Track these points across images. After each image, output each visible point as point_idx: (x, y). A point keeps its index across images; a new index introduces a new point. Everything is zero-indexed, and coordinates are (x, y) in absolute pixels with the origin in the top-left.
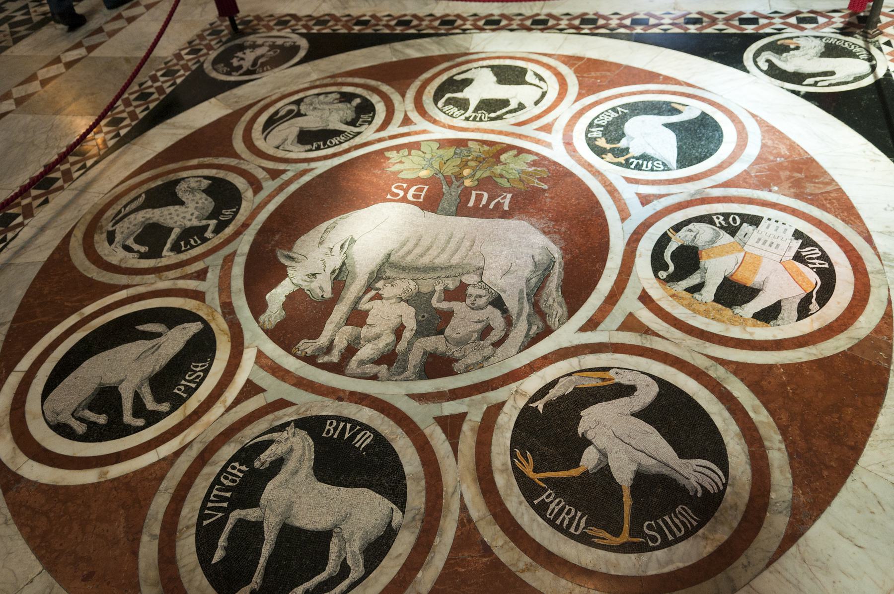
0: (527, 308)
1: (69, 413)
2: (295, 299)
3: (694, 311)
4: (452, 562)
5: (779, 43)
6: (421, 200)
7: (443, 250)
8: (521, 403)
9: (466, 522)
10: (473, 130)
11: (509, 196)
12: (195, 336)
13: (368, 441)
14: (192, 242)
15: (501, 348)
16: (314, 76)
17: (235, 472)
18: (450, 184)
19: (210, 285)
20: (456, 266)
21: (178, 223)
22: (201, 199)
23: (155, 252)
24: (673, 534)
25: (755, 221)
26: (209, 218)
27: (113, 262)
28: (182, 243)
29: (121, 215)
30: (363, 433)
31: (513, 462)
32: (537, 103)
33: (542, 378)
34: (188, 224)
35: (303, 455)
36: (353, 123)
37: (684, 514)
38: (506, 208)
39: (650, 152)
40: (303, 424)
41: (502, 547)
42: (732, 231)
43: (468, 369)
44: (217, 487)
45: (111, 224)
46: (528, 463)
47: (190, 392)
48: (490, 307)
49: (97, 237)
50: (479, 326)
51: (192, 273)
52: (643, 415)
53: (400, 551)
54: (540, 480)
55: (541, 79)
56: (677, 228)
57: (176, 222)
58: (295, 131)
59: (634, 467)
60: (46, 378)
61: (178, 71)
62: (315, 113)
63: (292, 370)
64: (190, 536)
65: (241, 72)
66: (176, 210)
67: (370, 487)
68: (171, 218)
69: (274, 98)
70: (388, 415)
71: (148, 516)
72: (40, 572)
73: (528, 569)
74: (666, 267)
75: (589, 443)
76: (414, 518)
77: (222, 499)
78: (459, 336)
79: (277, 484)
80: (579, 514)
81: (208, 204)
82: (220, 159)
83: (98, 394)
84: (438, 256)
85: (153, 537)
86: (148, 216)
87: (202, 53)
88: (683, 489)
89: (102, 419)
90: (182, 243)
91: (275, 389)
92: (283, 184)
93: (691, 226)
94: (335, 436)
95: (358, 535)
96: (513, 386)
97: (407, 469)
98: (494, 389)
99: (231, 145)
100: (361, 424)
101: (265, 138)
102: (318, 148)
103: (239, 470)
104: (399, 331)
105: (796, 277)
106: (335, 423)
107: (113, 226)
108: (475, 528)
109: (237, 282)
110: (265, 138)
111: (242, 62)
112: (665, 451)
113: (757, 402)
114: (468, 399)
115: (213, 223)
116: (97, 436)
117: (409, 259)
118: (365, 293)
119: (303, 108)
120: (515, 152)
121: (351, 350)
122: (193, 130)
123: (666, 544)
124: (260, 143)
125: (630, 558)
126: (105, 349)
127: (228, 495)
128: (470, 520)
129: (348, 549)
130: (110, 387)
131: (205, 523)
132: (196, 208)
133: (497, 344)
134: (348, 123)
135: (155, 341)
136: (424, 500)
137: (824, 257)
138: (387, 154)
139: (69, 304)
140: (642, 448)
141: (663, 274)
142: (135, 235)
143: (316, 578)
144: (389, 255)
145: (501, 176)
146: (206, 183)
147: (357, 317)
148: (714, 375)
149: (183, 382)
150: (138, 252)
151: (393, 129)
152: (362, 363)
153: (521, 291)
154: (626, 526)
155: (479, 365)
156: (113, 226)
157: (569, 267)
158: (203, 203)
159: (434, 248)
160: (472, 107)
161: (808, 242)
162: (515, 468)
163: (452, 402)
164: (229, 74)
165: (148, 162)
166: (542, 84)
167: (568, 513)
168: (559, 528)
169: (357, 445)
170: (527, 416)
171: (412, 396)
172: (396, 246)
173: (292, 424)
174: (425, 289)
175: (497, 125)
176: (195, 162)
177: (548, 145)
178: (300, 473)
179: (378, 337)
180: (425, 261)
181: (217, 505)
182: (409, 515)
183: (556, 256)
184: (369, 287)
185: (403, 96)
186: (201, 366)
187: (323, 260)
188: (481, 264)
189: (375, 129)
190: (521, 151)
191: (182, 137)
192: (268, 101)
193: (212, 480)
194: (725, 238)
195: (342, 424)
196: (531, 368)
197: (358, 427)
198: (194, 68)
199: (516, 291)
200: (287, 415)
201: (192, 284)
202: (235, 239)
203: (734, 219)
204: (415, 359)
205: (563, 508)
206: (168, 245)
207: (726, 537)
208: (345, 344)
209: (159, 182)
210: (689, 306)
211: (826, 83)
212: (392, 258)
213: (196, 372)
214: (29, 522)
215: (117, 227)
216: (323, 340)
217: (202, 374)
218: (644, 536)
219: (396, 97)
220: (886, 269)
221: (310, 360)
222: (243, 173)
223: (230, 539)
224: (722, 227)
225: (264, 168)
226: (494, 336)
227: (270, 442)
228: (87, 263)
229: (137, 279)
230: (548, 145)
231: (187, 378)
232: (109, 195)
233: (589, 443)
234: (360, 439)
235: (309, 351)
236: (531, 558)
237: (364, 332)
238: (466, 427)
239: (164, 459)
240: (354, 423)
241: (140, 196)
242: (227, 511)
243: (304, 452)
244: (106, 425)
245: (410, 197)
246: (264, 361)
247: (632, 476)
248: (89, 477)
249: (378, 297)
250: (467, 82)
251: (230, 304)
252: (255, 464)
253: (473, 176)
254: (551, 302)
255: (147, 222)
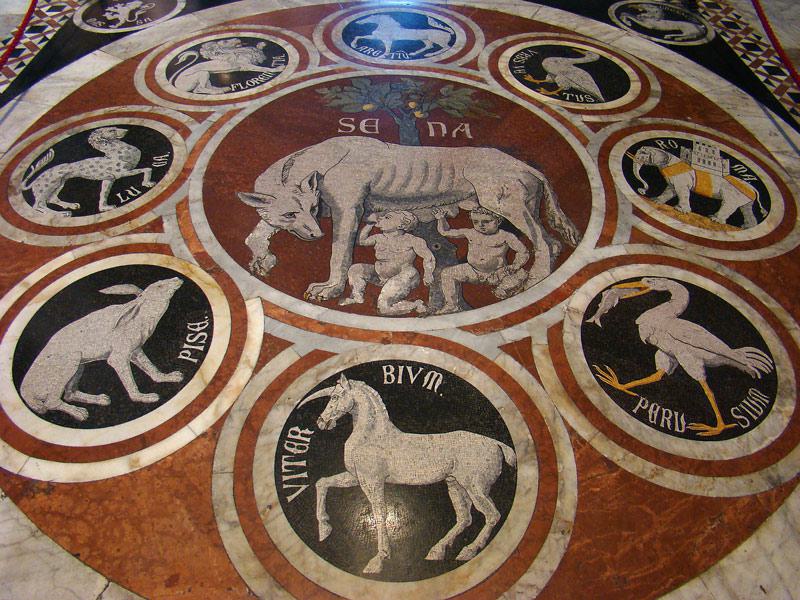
0: (538, 228)
1: (60, 395)
2: (282, 241)
3: (680, 220)
4: (584, 484)
5: (630, 6)
6: (377, 132)
7: (425, 179)
8: (579, 321)
9: (578, 443)
10: (400, 68)
11: (467, 125)
12: (177, 293)
13: (439, 381)
14: (130, 193)
15: (532, 271)
16: (204, 25)
17: (299, 437)
18: (400, 116)
19: (170, 233)
20: (447, 194)
21: (105, 175)
22: (122, 148)
23: (90, 208)
24: (757, 415)
25: (689, 144)
26: (139, 166)
27: (42, 224)
28: (119, 195)
29: (32, 174)
30: (429, 374)
31: (597, 378)
32: (451, 43)
33: (586, 294)
34: (118, 175)
35: (371, 407)
36: (266, 64)
37: (755, 399)
38: (470, 137)
39: (574, 86)
40: (358, 373)
41: (624, 459)
42: (677, 153)
43: (510, 293)
44: (284, 457)
45: (24, 183)
46: (609, 374)
47: (201, 356)
48: (501, 231)
49: (12, 199)
50: (500, 251)
51: (145, 226)
52: (686, 315)
53: (528, 487)
54: (629, 389)
55: (444, 25)
56: (633, 149)
57: (102, 174)
58: (204, 78)
59: (702, 364)
60: (11, 361)
61: (45, 27)
62: (219, 57)
63: (314, 317)
64: (277, 516)
65: (118, 25)
66: (98, 162)
67: (464, 429)
68: (94, 171)
69: (167, 46)
70: (448, 351)
71: (214, 502)
72: (107, 586)
73: (656, 473)
74: (643, 187)
75: (655, 349)
76: (526, 452)
77: (301, 470)
78: (484, 262)
79: (356, 442)
80: (676, 414)
81: (135, 154)
82: (129, 107)
83: (84, 372)
84: (422, 185)
85: (232, 524)
86: (67, 171)
87: (65, 9)
88: (745, 375)
89: (103, 400)
90: (119, 195)
91: (304, 342)
92: (213, 126)
93: (642, 149)
94: (400, 382)
95: (476, 479)
96: (563, 305)
97: (496, 404)
98: (546, 310)
99: (136, 92)
100: (422, 365)
101: (173, 84)
102: (238, 89)
103: (302, 435)
104: (417, 263)
105: (739, 188)
106: (392, 369)
107: (27, 185)
108: (592, 448)
109: (204, 231)
110: (173, 84)
111: (116, 16)
112: (720, 346)
113: (764, 293)
114: (524, 323)
115: (147, 171)
116: (105, 420)
117: (392, 189)
118: (360, 227)
119: (204, 54)
120: (452, 86)
121: (372, 290)
122: (86, 82)
123: (755, 424)
124: (168, 88)
125: (733, 443)
126: (72, 320)
127: (303, 463)
128: (583, 442)
129: (472, 497)
130: (97, 362)
131: (290, 499)
132: (120, 158)
133: (528, 265)
134: (259, 65)
135: (130, 304)
136: (527, 431)
137: (750, 172)
138: (318, 91)
139: (6, 275)
140: (700, 345)
141: (642, 191)
142: (58, 192)
143: (451, 531)
144: (368, 188)
145: (451, 108)
146: (121, 132)
147: (362, 254)
148: (723, 274)
149: (186, 346)
150: (68, 209)
151: (314, 68)
152: (392, 301)
153: (525, 214)
154: (718, 416)
155: (520, 288)
156: (27, 185)
157: (556, 191)
158: (126, 152)
159: (414, 177)
160: (388, 49)
161: (734, 161)
162: (602, 384)
163: (510, 329)
164: (106, 27)
165: (43, 116)
166: (446, 28)
167: (667, 415)
168: (665, 430)
169: (429, 387)
170: (587, 331)
171: (464, 328)
172: (372, 178)
173: (342, 375)
174: (424, 219)
175: (421, 62)
176: (100, 112)
177: (482, 81)
178: (378, 427)
179: (396, 272)
180: (411, 189)
181: (294, 476)
182: (520, 449)
183: (542, 179)
184: (362, 223)
185: (311, 39)
186: (201, 326)
187: (293, 198)
188: (473, 190)
189: (294, 69)
190: (457, 85)
191: (74, 89)
192: (161, 49)
193: (274, 450)
194: (674, 160)
195: (401, 368)
196: (571, 285)
197: (421, 369)
198: (63, 23)
199: (520, 213)
200: (332, 367)
201: (149, 238)
202: (180, 186)
203: (672, 144)
204: (449, 290)
205: (660, 412)
206: (103, 199)
207: (793, 408)
208: (363, 283)
209: (65, 136)
210: (676, 217)
211: (680, 39)
212: (373, 190)
213: (197, 333)
214: (64, 530)
215: (33, 185)
216: (335, 280)
217: (205, 334)
218: (736, 421)
219: (303, 40)
220: (795, 180)
221: (331, 303)
222: (161, 119)
223: (329, 509)
224: (665, 149)
225: (184, 112)
226: (521, 257)
227: (326, 399)
228: (10, 228)
229: (79, 239)
230: (482, 81)
231: (188, 339)
232: (10, 152)
233: (655, 349)
234: (430, 380)
235: (325, 294)
236: (655, 463)
237: (378, 268)
238: (536, 352)
239: (204, 435)
240: (416, 366)
241: (47, 151)
242: (312, 481)
243: (370, 401)
244: (111, 405)
245: (362, 127)
246: (274, 312)
247: (703, 371)
248: (117, 467)
249: (376, 231)
250: (370, 28)
251: (205, 254)
252: (319, 426)
253: (421, 107)
254: (557, 222)
255: (67, 178)
